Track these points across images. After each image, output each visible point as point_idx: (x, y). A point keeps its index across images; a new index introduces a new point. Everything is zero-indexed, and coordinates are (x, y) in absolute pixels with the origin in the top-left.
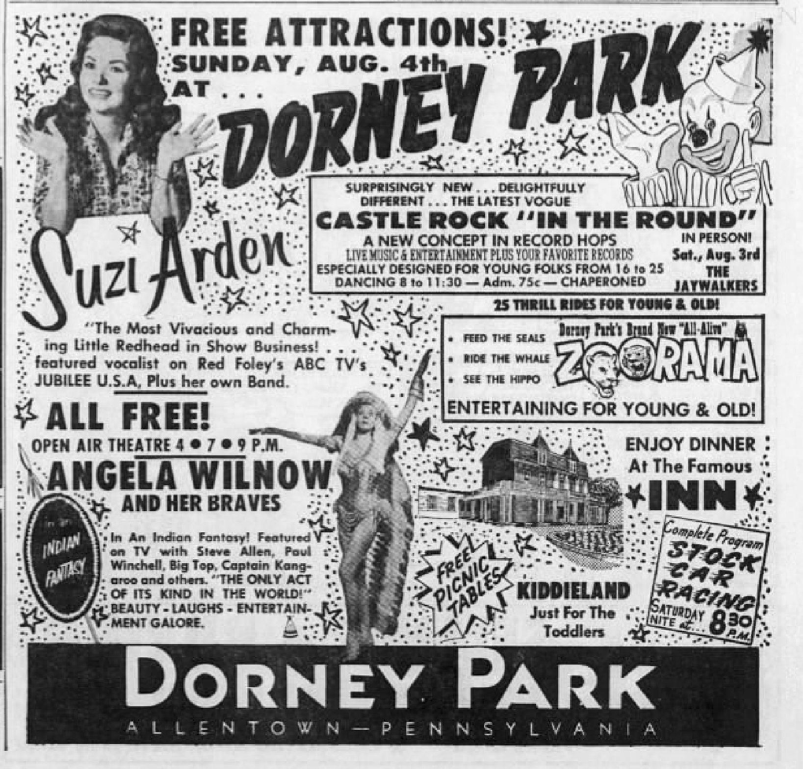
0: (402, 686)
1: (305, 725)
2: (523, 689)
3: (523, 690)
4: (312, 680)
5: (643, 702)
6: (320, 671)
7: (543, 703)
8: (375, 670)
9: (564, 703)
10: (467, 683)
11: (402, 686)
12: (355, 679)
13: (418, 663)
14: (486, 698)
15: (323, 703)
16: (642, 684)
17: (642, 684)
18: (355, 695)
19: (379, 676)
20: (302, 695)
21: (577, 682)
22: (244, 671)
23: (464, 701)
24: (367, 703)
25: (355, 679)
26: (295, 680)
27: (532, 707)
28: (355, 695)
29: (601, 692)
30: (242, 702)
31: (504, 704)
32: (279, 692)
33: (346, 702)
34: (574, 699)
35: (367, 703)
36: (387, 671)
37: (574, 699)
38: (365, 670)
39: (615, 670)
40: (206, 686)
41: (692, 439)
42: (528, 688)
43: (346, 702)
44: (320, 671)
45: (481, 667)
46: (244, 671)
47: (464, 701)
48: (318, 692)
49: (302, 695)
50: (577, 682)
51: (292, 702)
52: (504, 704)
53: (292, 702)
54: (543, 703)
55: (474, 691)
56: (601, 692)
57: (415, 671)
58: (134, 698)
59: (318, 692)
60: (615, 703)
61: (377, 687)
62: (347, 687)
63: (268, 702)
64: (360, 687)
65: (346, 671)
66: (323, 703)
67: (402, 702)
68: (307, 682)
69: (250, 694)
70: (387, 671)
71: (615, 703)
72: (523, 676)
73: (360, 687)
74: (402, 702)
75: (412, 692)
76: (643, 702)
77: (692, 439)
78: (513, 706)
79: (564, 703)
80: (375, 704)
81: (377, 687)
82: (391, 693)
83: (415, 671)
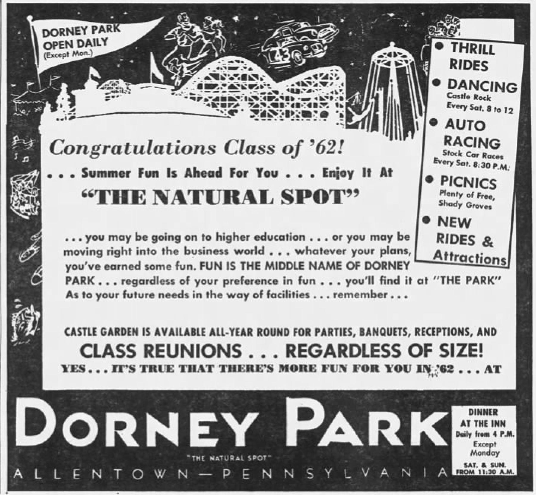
0: (240, 430)
1: (160, 472)
2: (341, 431)
3: (340, 431)
4: (166, 423)
5: (438, 440)
6: (174, 418)
7: (356, 441)
8: (219, 417)
9: (374, 441)
10: (294, 427)
11: (240, 430)
12: (202, 424)
13: (253, 411)
14: (309, 438)
15: (176, 442)
16: (438, 426)
17: (438, 426)
18: (202, 436)
19: (222, 422)
20: (159, 437)
21: (384, 425)
22: (112, 418)
23: (292, 441)
24: (212, 443)
25: (202, 424)
26: (153, 425)
27: (348, 445)
28: (202, 436)
29: (404, 433)
30: (110, 442)
31: (324, 442)
32: (140, 434)
33: (195, 442)
34: (382, 438)
35: (212, 443)
36: (229, 418)
37: (382, 437)
38: (211, 417)
39: (416, 416)
40: (80, 430)
41: (366, 263)
42: (344, 429)
43: (195, 442)
44: (174, 418)
45: (305, 414)
46: (112, 418)
47: (292, 441)
48: (172, 434)
49: (159, 437)
50: (384, 425)
51: (151, 442)
52: (324, 442)
53: (151, 442)
54: (356, 441)
55: (300, 433)
56: (404, 433)
57: (251, 418)
58: (23, 440)
59: (172, 434)
60: (415, 441)
61: (220, 430)
62: (195, 430)
63: (131, 442)
64: (206, 430)
65: (195, 418)
66: (176, 442)
67: (240, 441)
68: (164, 427)
69: (116, 434)
70: (229, 418)
71: (415, 441)
72: (340, 420)
73: (206, 430)
74: (240, 441)
75: (249, 433)
76: (438, 440)
77: (366, 263)
78: (332, 444)
79: (374, 441)
80: (218, 444)
81: (220, 430)
82: (232, 435)
83: (251, 418)
